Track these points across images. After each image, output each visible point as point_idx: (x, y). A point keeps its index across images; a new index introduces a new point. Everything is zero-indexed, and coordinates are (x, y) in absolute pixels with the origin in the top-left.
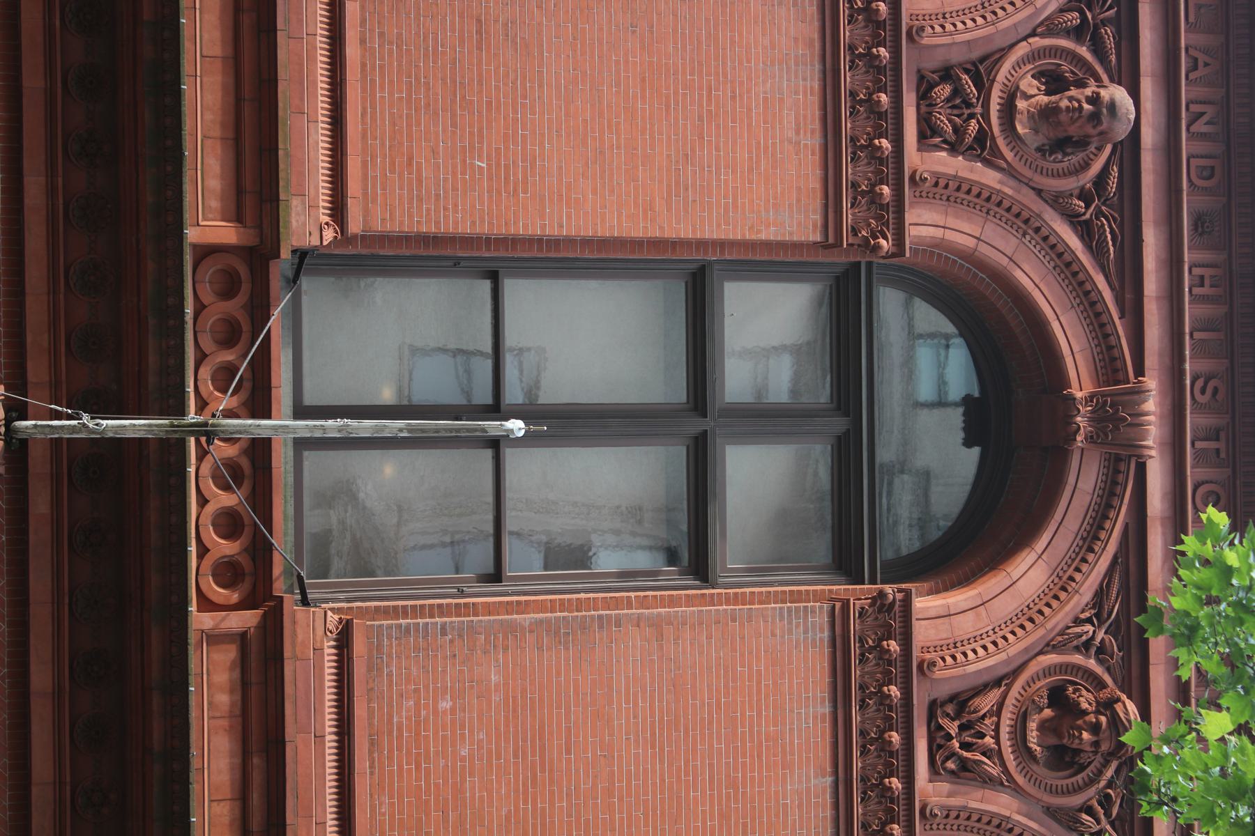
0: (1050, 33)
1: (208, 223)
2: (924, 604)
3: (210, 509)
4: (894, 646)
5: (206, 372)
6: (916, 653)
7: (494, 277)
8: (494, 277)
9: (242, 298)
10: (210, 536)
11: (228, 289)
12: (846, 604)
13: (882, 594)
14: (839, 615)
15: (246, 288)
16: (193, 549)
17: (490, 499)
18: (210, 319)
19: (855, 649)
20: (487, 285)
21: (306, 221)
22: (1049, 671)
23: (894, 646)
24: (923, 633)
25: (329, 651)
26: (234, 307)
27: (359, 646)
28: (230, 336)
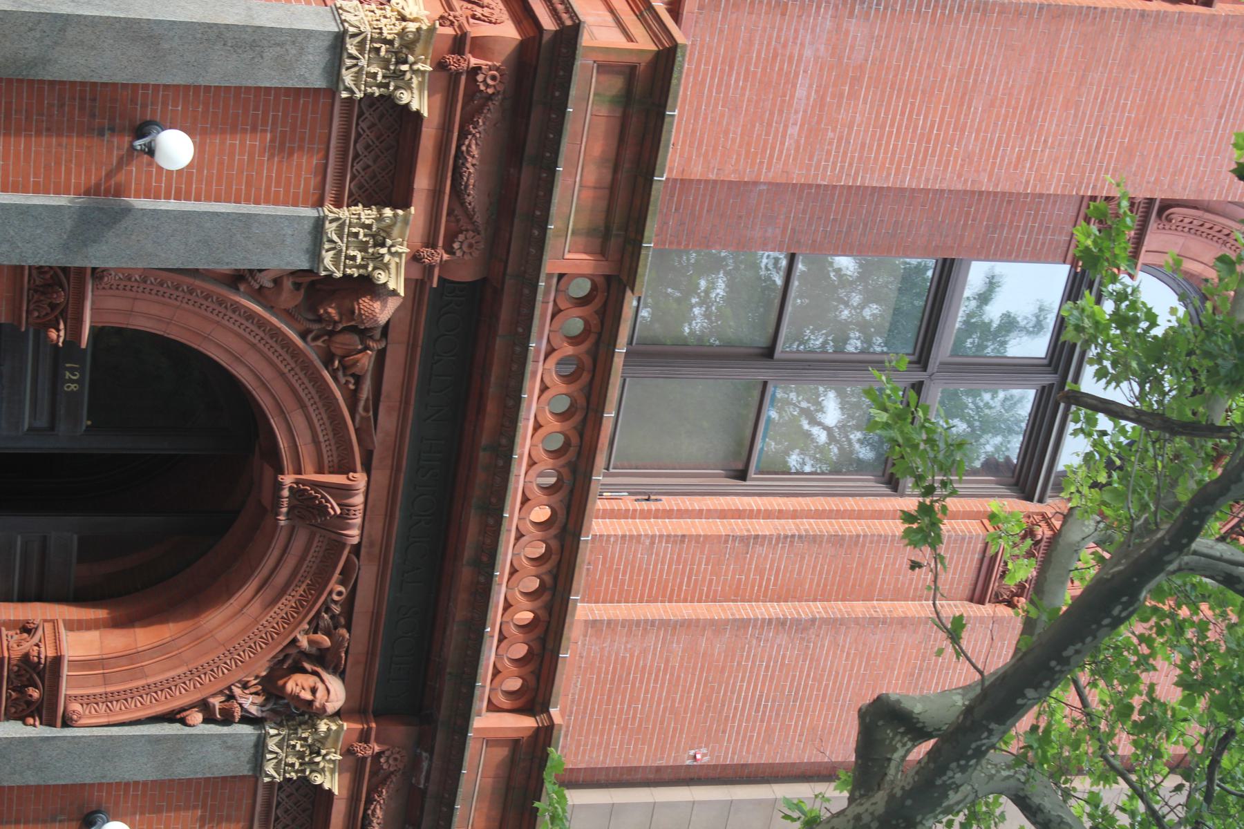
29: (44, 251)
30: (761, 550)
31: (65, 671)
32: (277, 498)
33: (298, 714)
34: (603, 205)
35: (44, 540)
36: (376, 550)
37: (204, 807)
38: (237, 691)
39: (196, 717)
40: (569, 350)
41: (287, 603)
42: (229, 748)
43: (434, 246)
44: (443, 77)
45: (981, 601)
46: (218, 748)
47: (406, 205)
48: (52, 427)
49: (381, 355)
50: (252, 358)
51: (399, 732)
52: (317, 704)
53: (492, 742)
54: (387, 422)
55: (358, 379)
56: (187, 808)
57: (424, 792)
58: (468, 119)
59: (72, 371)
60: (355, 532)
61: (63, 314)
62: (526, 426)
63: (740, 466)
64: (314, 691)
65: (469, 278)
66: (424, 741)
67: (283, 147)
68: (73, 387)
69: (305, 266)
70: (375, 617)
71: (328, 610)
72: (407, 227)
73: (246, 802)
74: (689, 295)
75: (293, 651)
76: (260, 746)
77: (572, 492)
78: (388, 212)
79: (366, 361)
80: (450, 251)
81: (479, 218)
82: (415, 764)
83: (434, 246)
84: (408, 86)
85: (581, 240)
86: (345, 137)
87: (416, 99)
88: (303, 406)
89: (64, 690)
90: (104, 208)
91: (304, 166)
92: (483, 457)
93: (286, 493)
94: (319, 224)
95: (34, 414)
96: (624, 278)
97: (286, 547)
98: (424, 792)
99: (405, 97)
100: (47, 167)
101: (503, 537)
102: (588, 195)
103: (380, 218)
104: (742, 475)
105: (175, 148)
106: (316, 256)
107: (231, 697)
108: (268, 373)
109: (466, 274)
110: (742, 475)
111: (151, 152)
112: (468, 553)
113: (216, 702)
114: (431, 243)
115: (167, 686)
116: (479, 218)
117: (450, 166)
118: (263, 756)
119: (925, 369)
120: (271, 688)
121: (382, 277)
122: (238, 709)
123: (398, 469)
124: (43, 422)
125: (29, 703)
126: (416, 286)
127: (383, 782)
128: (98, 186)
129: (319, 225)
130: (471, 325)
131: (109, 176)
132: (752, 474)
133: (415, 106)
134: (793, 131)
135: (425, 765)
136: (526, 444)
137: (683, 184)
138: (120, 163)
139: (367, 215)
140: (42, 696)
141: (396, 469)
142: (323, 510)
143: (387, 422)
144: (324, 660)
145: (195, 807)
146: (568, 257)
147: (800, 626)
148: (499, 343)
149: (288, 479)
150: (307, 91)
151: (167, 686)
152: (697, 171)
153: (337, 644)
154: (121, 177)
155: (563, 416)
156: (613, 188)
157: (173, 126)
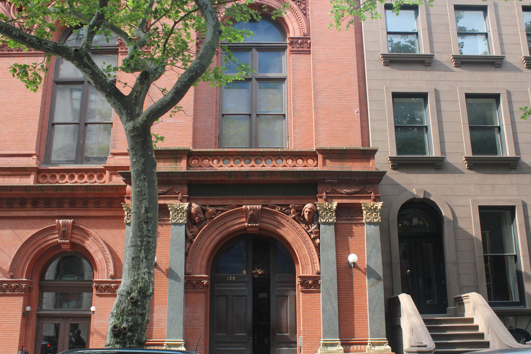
0: (9, 11)
1: (30, 181)
2: (291, 35)
3: (87, 181)
4: (300, 41)
5: (61, 182)
6: (302, 36)
7: (53, 124)
8: (53, 124)
9: (47, 174)
10: (83, 181)
11: (45, 177)
12: (291, 51)
13: (289, 43)
14: (293, 52)
15: (45, 174)
16: (86, 184)
17: (98, 125)
18: (50, 180)
19: (300, 49)
20: (56, 126)
21: (32, 162)
22: (14, 12)
23: (300, 41)
24: (298, 35)
25: (116, 157)
26: (48, 176)
27: (116, 151)
28: (54, 177)
29: (180, 287)
30: (297, 107)
31: (305, 275)
32: (251, 227)
33: (314, 215)
34: (169, 160)
35: (277, 282)
36: (267, 201)
37: (348, 236)
38: (310, 231)
39: (318, 241)
40: (221, 162)
41: (282, 221)
42: (325, 231)
43: (371, 196)
44: (328, 200)
45: (310, 51)
46: (328, 234)
47: (361, 204)
48: (245, 282)
49: (210, 206)
50: (213, 236)
51: (319, 189)
52: (309, 210)
53: (324, 164)
54: (230, 202)
55: (217, 211)
56: (348, 240)
57: (338, 180)
58: (338, 193)
59: (229, 278)
60: (258, 207)
61: (200, 281)
62: (243, 169)
63: (282, 116)
64: (306, 212)
65: (187, 188)
66: (323, 182)
67: (351, 234)
68: (234, 278)
69: (184, 226)
70: (287, 199)
71: (284, 210)
72: (174, 203)
73: (346, 225)
74: (237, 138)
75: (297, 218)
76: (324, 223)
77: (251, 155)
78: (363, 208)
79: (210, 210)
80: (371, 193)
81: (170, 188)
82: (329, 183)
83: (178, 197)
84: (377, 207)
85: (178, 164)
86: (347, 220)
87: (335, 204)
88: (226, 223)
89: (311, 275)
90: (370, 272)
91: (355, 228)
92: (233, 178)
93: (250, 225)
94: (367, 223)
95: (242, 286)
96: (187, 152)
97: (268, 223)
98: (338, 180)
99: (334, 207)
100: (161, 286)
101: (254, 170)
102: (166, 164)
103: (365, 210)
104: (284, 115)
105: (352, 258)
106: (181, 224)
107: (311, 232)
108: (217, 232)
109: (186, 189)
110: (284, 115)
111: (354, 263)
112: (261, 178)
113: (312, 236)
114: (176, 198)
115: (309, 249)
116: (362, 188)
117: (349, 196)
118: (327, 222)
119: (252, 79)
120: (308, 223)
121: (185, 208)
122: (315, 230)
123: (243, 198)
124: (244, 284)
125: (314, 283)
126: (188, 200)
127: (336, 191)
128: (166, 275)
129: (367, 223)
130: (197, 186)
131: (164, 273)
132: (284, 113)
133: (336, 205)
134: (180, 121)
135: (329, 180)
136: (236, 168)
137: (195, 143)
138: (161, 270)
139: (364, 212)
140: (311, 280)
141: (243, 199)
142: (252, 215)
143: (230, 202)
144: (299, 211)
145: (348, 238)
146: (182, 166)
147: (316, 93)
148: (201, 179)
149: (246, 224)
150: (335, 229)
151: (309, 249)
152: (190, 140)
153: (294, 207)
154: (164, 270)
155: (272, 160)
156: (165, 159)
157: (347, 259)
